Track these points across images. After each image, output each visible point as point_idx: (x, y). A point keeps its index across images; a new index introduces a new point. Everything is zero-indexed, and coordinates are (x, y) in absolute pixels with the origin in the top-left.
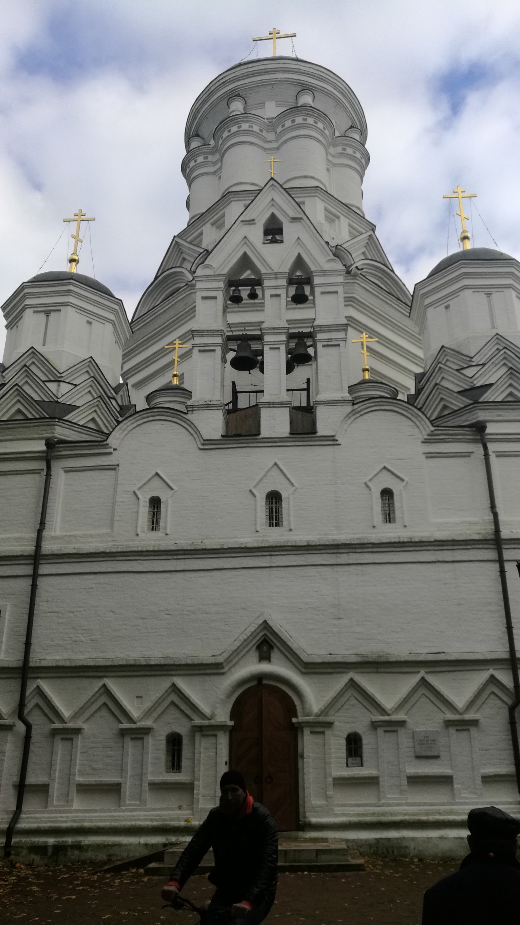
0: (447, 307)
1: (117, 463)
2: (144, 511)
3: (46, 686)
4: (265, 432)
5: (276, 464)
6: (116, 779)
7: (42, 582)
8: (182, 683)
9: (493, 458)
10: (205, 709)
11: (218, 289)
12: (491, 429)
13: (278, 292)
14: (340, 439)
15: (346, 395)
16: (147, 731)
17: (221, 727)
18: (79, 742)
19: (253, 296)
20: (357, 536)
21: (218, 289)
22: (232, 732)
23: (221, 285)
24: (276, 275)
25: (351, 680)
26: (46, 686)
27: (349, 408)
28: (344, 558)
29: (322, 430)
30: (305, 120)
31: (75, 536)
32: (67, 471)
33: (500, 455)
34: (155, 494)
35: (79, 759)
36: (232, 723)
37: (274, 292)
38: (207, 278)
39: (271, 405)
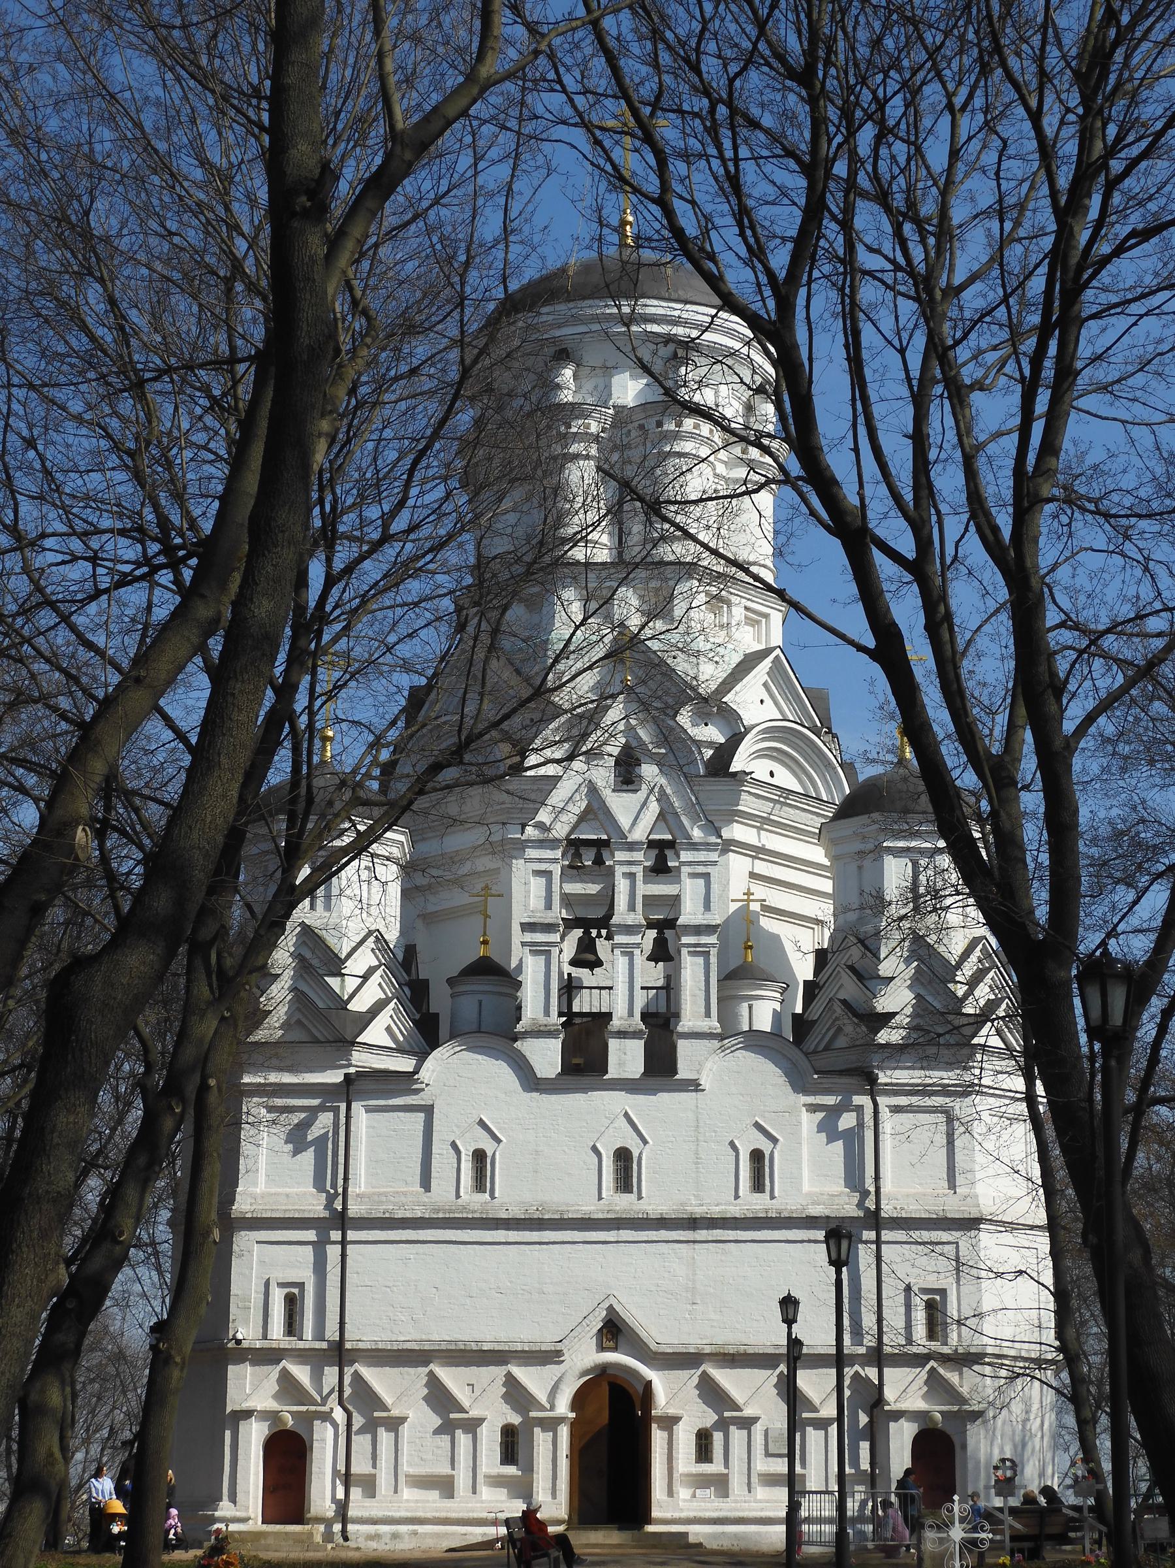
0: (860, 868)
1: (430, 1102)
2: (467, 1166)
3: (367, 1373)
4: (613, 1072)
5: (626, 1115)
6: (446, 1470)
7: (350, 1248)
8: (519, 1372)
9: (885, 1113)
10: (542, 1397)
11: (555, 860)
12: (883, 1078)
13: (633, 869)
14: (704, 1082)
15: (713, 1024)
16: (480, 1421)
17: (561, 1420)
18: (405, 1429)
19: (599, 861)
20: (717, 1209)
21: (555, 860)
22: (574, 1425)
23: (558, 853)
24: (632, 847)
25: (704, 1372)
26: (367, 1373)
27: (716, 1043)
28: (702, 1234)
29: (683, 1073)
30: (679, 425)
31: (385, 1194)
32: (369, 1110)
33: (896, 1109)
34: (481, 1146)
35: (405, 1448)
36: (573, 1415)
37: (626, 869)
38: (541, 844)
39: (622, 1034)
